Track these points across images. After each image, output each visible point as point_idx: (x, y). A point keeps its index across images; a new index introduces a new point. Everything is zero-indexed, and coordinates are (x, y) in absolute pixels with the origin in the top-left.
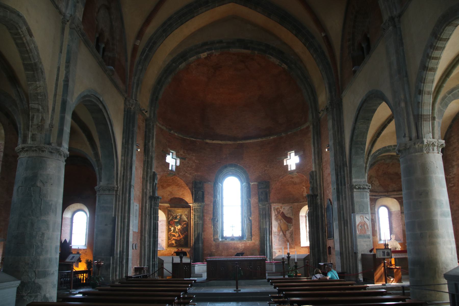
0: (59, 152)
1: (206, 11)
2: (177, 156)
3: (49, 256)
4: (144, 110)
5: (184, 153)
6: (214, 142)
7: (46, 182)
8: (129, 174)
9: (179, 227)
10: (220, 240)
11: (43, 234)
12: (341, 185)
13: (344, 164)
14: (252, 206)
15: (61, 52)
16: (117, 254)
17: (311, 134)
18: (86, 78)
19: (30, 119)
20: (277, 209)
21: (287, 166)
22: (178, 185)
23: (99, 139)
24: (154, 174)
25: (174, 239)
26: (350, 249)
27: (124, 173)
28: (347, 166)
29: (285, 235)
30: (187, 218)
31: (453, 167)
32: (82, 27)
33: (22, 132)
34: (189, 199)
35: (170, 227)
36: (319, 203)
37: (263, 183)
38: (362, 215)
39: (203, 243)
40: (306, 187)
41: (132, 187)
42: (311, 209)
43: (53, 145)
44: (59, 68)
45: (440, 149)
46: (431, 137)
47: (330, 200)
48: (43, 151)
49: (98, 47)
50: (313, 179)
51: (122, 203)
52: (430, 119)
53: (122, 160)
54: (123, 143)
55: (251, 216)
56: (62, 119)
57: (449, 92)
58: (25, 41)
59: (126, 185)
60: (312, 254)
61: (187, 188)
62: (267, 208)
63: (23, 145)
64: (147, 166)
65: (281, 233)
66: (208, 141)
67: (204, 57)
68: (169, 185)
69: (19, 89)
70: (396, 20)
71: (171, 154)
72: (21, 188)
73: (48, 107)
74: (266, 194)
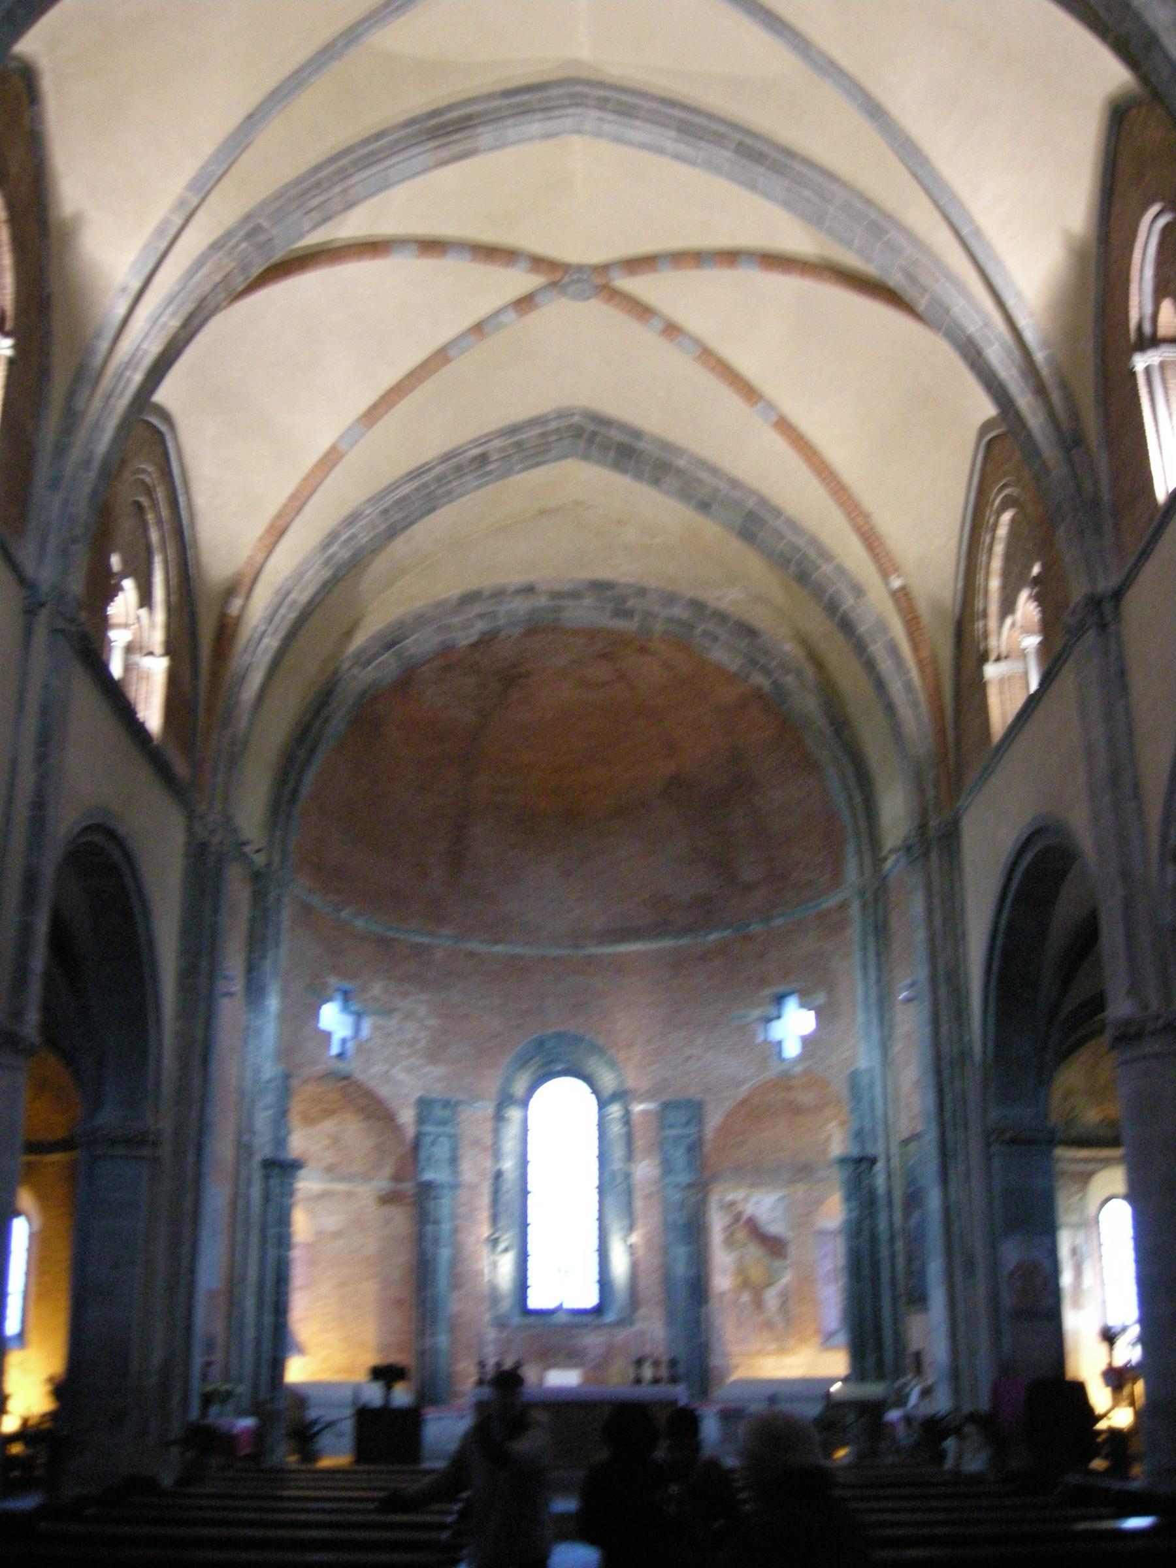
6: (499, 948)
15: (21, 708)
17: (854, 932)
39: (453, 1330)
42: (851, 1211)
44: (14, 762)
65: (746, 1297)
66: (473, 946)
67: (466, 642)
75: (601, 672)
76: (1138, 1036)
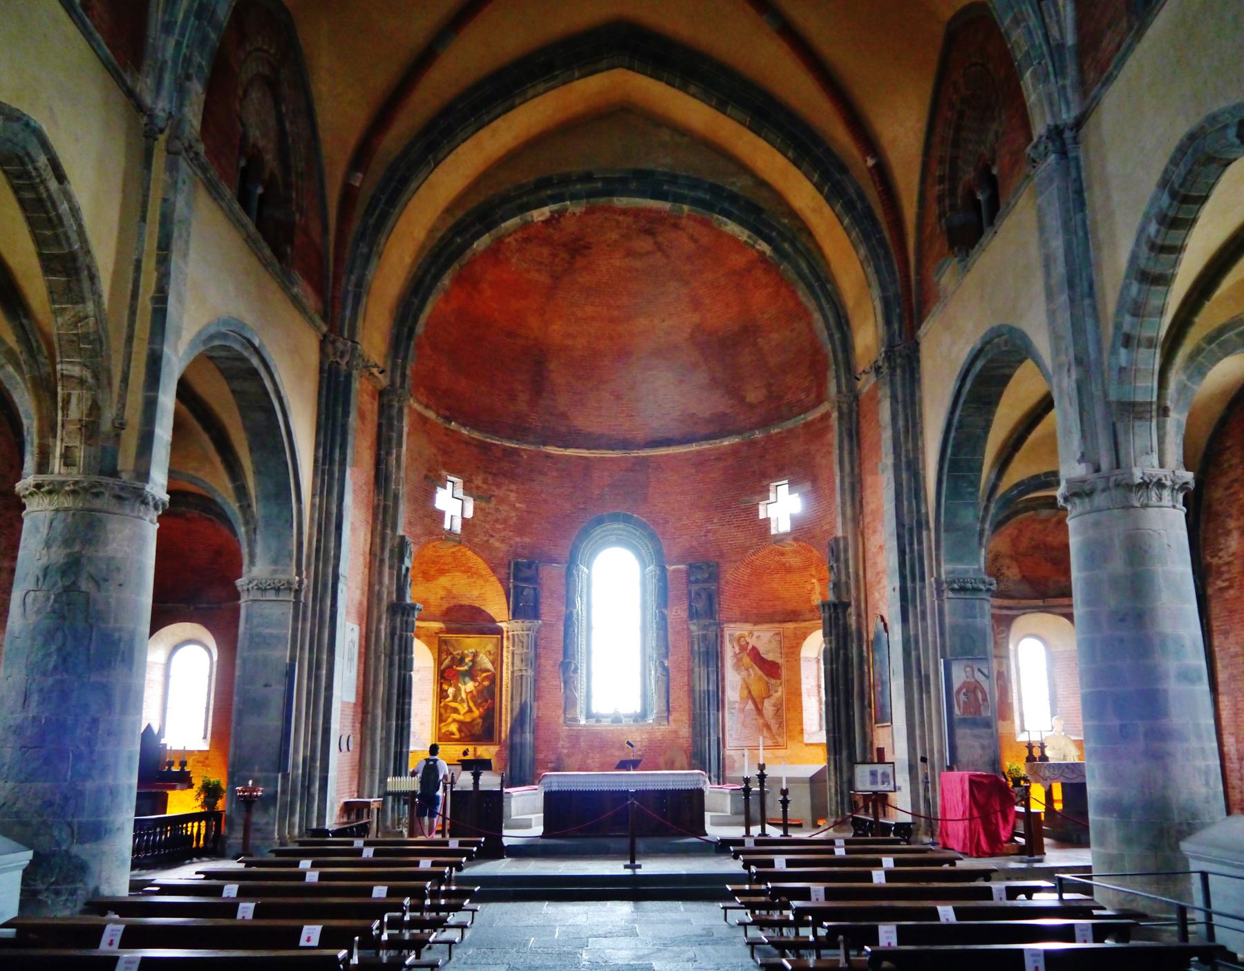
0: (141, 498)
1: (546, 91)
2: (467, 490)
3: (110, 780)
4: (376, 366)
5: (485, 482)
6: (569, 452)
7: (106, 580)
8: (332, 545)
9: (470, 686)
10: (583, 722)
11: (95, 721)
12: (914, 580)
13: (921, 524)
14: (670, 630)
15: (143, 219)
16: (295, 766)
17: (834, 437)
18: (212, 290)
19: (60, 405)
20: (739, 640)
21: (767, 520)
22: (469, 571)
23: (251, 450)
24: (403, 543)
25: (454, 720)
26: (936, 755)
27: (318, 541)
28: (928, 529)
29: (759, 711)
30: (493, 663)
31: (1228, 533)
32: (201, 148)
33: (36, 441)
34: (496, 606)
35: (445, 687)
36: (854, 627)
37: (700, 568)
38: (970, 663)
40: (820, 580)
41: (341, 578)
42: (830, 642)
43: (125, 476)
45: (1181, 496)
46: (1156, 463)
47: (882, 619)
48: (97, 495)
49: (244, 198)
50: (837, 560)
51: (313, 625)
52: (1154, 414)
53: (313, 505)
54: (316, 461)
55: (667, 657)
56: (150, 407)
57: (1210, 339)
58: (45, 195)
59: (325, 575)
60: (832, 767)
61: (494, 579)
62: (711, 635)
63: (41, 478)
64: (384, 518)
65: (750, 705)
66: (551, 450)
67: (541, 219)
68: (442, 572)
69: (25, 321)
70: (1068, 135)
71: (449, 485)
72: (32, 594)
73: (109, 371)
74: (710, 598)
75: (644, 244)
76: (1090, 494)
